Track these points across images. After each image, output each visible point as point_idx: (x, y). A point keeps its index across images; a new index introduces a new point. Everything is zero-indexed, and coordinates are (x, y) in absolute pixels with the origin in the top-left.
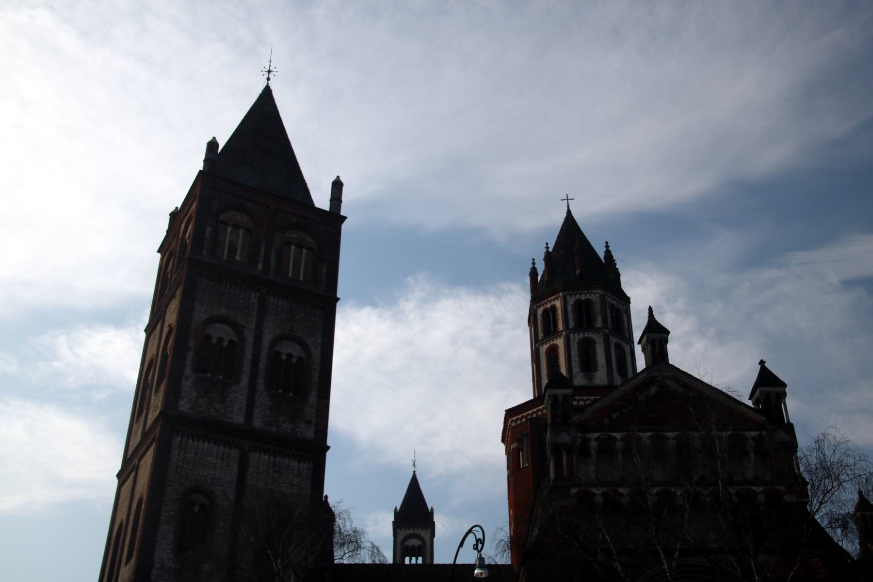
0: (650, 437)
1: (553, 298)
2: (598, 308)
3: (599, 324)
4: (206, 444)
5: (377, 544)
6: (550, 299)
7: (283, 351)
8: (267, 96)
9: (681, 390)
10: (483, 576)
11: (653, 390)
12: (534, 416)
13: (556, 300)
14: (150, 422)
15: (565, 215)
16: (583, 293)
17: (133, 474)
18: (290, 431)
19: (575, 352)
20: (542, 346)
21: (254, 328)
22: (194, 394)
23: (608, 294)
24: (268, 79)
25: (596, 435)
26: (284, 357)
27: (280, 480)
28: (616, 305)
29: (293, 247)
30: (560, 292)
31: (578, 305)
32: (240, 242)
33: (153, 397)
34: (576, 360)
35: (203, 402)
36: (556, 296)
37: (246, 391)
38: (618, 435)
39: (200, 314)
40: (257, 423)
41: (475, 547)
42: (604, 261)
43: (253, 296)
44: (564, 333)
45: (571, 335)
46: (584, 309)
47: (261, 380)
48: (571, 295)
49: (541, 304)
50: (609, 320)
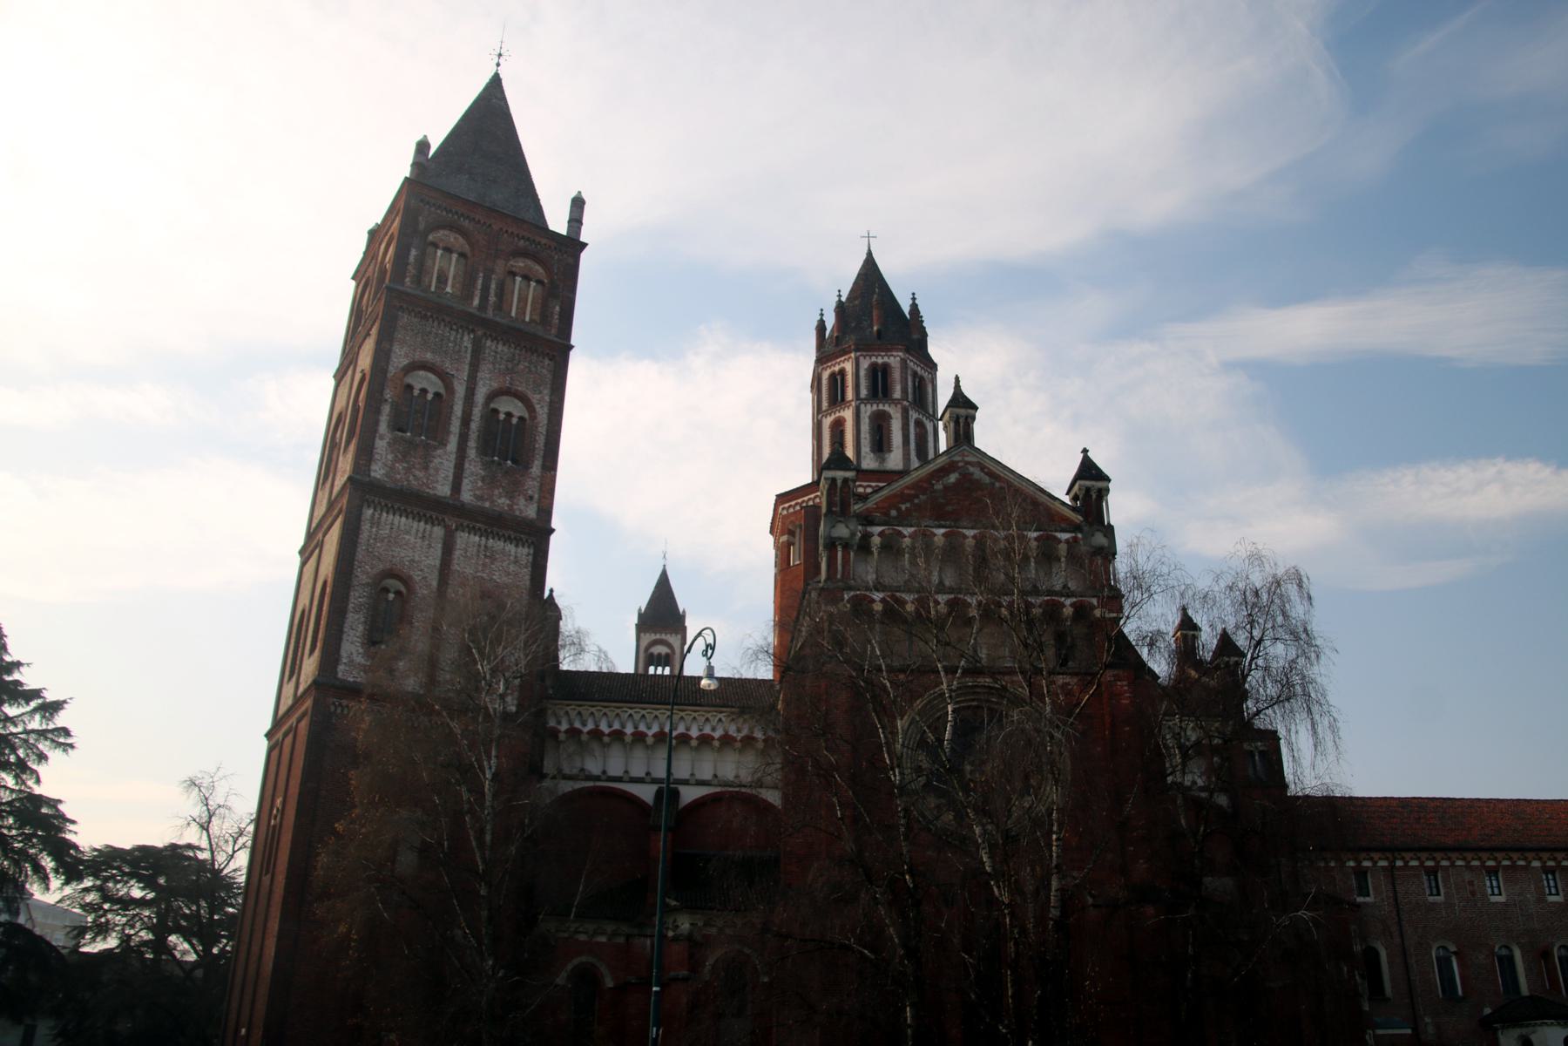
1: (843, 358)
2: (896, 375)
3: (897, 394)
4: (403, 519)
5: (604, 648)
6: (838, 360)
7: (501, 409)
8: (495, 84)
9: (987, 479)
10: (712, 688)
11: (953, 478)
12: (811, 503)
13: (846, 362)
14: (336, 489)
15: (864, 256)
17: (317, 551)
18: (506, 508)
21: (465, 379)
22: (390, 457)
23: (911, 358)
24: (498, 65)
25: (879, 529)
26: (502, 417)
27: (493, 566)
28: (919, 373)
29: (518, 279)
30: (850, 352)
31: (874, 369)
32: (452, 269)
33: (341, 458)
34: (865, 438)
35: (401, 468)
36: (846, 357)
37: (453, 456)
38: (907, 531)
39: (400, 358)
40: (466, 496)
41: (705, 654)
42: (908, 316)
43: (466, 338)
44: (853, 403)
45: (862, 406)
46: (880, 374)
47: (472, 444)
48: (865, 358)
50: (910, 390)
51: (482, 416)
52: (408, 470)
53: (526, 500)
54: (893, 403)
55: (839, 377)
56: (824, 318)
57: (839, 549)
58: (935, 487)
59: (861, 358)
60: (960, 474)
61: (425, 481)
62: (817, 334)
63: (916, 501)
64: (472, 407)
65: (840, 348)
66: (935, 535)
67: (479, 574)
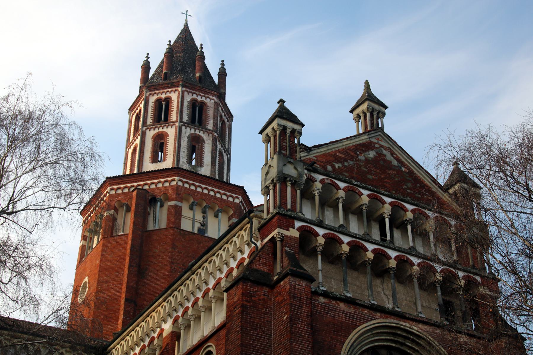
0: (369, 196)
1: (170, 90)
3: (210, 126)
6: (166, 90)
9: (395, 163)
11: (372, 154)
13: (172, 93)
15: (183, 27)
16: (200, 95)
19: (184, 143)
20: (150, 130)
23: (221, 104)
25: (320, 177)
30: (178, 86)
31: (194, 104)
34: (184, 152)
36: (174, 89)
38: (342, 185)
44: (177, 124)
45: (184, 128)
46: (197, 108)
49: (155, 93)
54: (207, 132)
55: (164, 103)
56: (149, 60)
57: (289, 184)
58: (359, 157)
59: (186, 93)
60: (377, 153)
62: (142, 71)
63: (346, 164)
65: (165, 82)
66: (362, 194)
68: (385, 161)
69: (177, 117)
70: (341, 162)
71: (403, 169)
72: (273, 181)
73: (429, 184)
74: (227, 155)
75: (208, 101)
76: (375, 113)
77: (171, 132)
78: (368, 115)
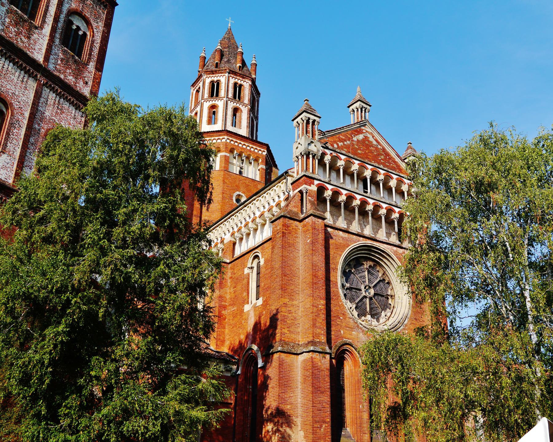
7: (74, 22)
13: (221, 77)
18: (72, 83)
31: (235, 84)
35: (13, 30)
36: (223, 75)
44: (225, 99)
45: (229, 102)
46: (238, 88)
47: (58, 35)
51: (65, 21)
52: (18, 34)
53: (84, 83)
55: (216, 84)
61: (27, 45)
63: (345, 143)
64: (60, 13)
67: (53, 118)
68: (368, 141)
69: (225, 94)
70: (342, 142)
71: (379, 147)
72: (301, 153)
73: (394, 157)
74: (256, 120)
75: (244, 84)
76: (363, 109)
77: (220, 104)
78: (359, 110)
